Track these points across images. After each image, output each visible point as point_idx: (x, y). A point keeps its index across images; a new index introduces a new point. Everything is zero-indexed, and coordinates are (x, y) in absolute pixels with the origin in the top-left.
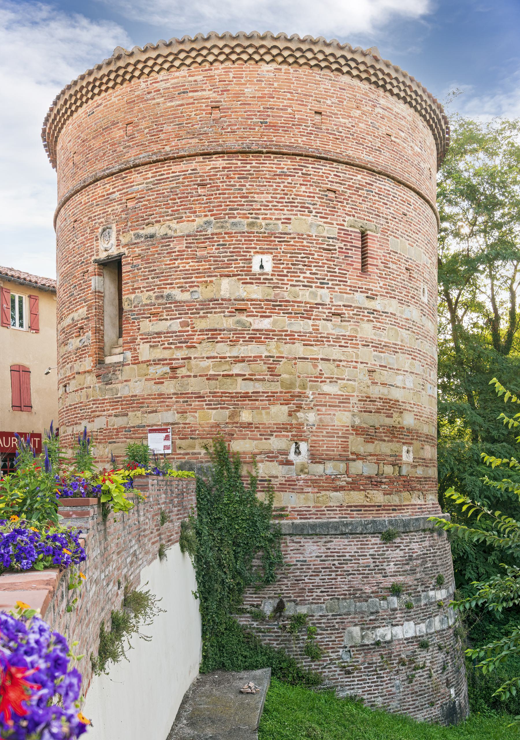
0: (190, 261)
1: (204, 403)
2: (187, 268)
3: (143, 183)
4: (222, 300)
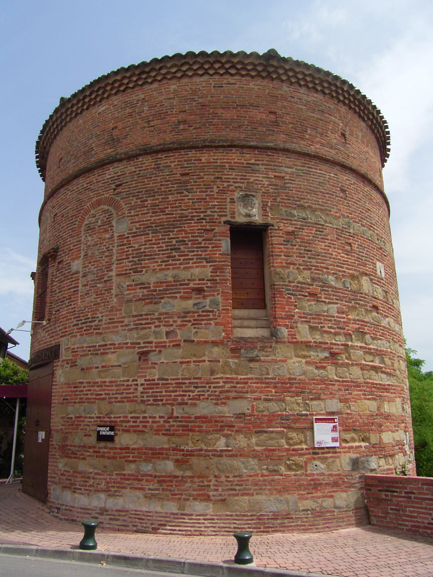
0: (340, 251)
1: (361, 393)
2: (339, 257)
3: (292, 168)
4: (366, 294)
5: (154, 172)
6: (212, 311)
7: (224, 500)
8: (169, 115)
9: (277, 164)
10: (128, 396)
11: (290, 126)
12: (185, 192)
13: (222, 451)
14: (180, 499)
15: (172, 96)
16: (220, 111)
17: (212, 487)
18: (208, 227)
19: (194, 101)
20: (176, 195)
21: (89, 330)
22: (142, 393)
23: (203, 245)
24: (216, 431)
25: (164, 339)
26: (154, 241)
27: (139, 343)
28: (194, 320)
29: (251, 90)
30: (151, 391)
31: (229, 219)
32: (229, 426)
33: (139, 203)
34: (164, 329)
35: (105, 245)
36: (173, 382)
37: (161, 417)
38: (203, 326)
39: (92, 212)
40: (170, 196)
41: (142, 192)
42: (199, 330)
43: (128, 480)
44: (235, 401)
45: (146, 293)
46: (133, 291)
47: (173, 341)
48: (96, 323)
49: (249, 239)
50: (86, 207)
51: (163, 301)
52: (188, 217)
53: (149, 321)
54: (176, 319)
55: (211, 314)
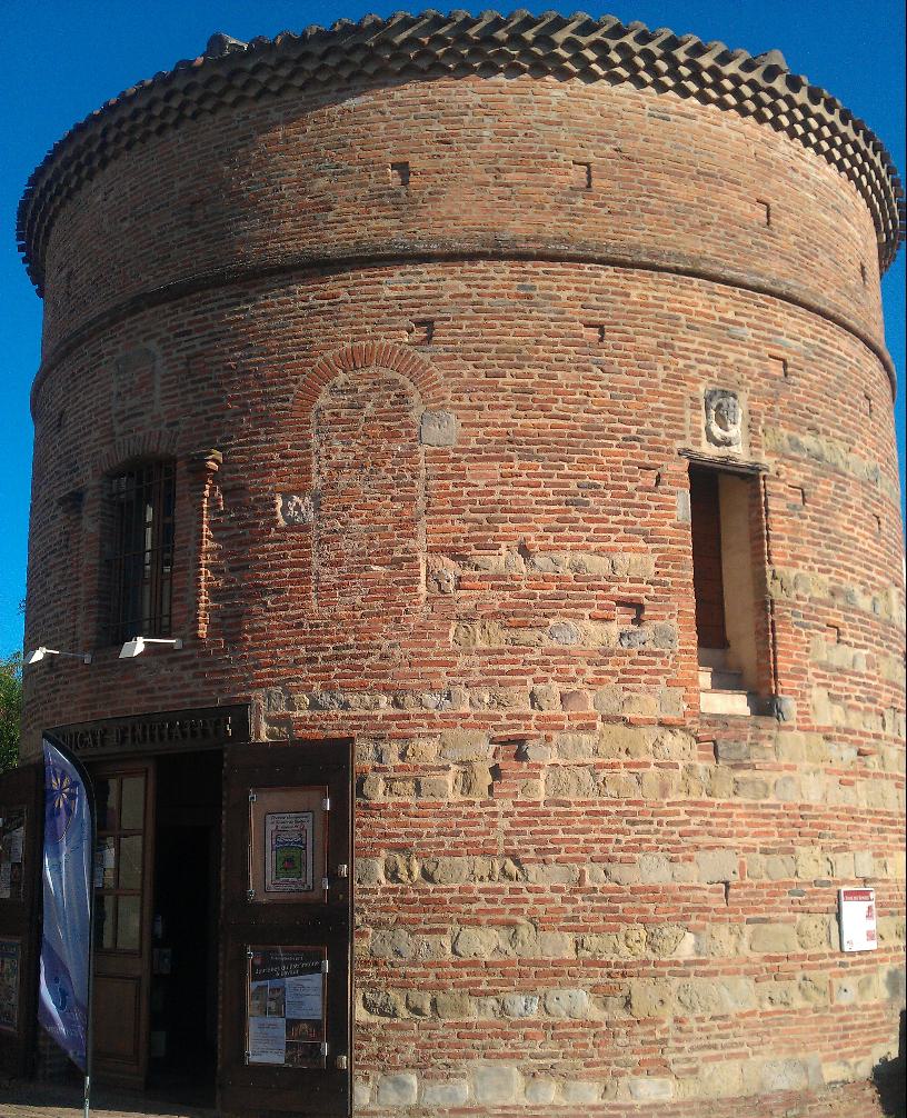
5: (519, 306)
6: (660, 654)
7: (694, 1071)
8: (552, 165)
9: (772, 326)
10: (473, 839)
11: (793, 238)
12: (594, 367)
13: (687, 963)
14: (603, 1075)
15: (553, 116)
16: (665, 180)
17: (672, 1044)
18: (647, 461)
19: (607, 142)
20: (574, 372)
22: (507, 833)
23: (636, 500)
24: (675, 919)
25: (557, 710)
26: (524, 479)
27: (498, 718)
28: (624, 672)
29: (721, 138)
30: (528, 829)
31: (690, 446)
32: (700, 910)
34: (557, 688)
35: (393, 470)
36: (583, 809)
37: (555, 890)
38: (643, 685)
39: (342, 377)
40: (559, 374)
41: (489, 351)
42: (634, 695)
43: (480, 1037)
44: (710, 854)
47: (578, 717)
49: (721, 494)
50: (320, 359)
51: (552, 622)
52: (602, 429)
53: (518, 667)
54: (584, 666)
55: (658, 660)
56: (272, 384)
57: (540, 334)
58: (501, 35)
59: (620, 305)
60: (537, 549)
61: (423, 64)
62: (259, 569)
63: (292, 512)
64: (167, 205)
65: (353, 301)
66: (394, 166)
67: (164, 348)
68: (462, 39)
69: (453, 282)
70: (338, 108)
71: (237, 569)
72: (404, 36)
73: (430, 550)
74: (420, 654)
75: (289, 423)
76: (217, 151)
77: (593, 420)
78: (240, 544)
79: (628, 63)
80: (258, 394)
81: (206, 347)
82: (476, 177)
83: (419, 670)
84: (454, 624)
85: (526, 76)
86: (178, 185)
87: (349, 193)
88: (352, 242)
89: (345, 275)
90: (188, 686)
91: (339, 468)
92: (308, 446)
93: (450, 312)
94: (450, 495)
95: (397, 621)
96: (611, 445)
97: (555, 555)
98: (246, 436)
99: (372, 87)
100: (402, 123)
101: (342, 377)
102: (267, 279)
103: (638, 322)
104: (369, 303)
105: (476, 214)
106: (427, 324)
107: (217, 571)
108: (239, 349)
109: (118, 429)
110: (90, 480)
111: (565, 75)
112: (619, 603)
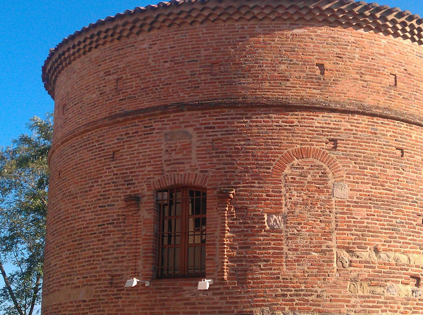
5: (372, 138)
12: (400, 168)
15: (382, 52)
21: (304, 305)
23: (416, 230)
26: (376, 217)
33: (358, 169)
39: (296, 161)
40: (388, 170)
41: (360, 156)
45: (371, 273)
46: (358, 269)
48: (314, 297)
50: (285, 151)
51: (388, 284)
52: (403, 197)
54: (400, 305)
56: (261, 160)
57: (380, 151)
58: (367, 13)
59: (408, 141)
60: (381, 250)
61: (332, 20)
62: (256, 249)
63: (272, 223)
64: (197, 61)
65: (301, 126)
66: (317, 65)
67: (198, 133)
68: (351, 12)
69: (344, 123)
70: (290, 32)
71: (244, 248)
72: (327, 6)
73: (338, 247)
74: (335, 296)
75: (270, 180)
76: (227, 41)
77: (400, 192)
78: (245, 235)
79: (412, 33)
80: (254, 164)
81: (223, 136)
82: (353, 75)
83: (334, 303)
84: (349, 283)
85: (372, 31)
86: (203, 53)
87: (297, 74)
88: (299, 98)
89: (297, 113)
90: (216, 303)
91: (295, 204)
92: (281, 192)
93: (344, 136)
94: (346, 222)
95: (324, 279)
96: (407, 204)
97: (389, 254)
98: (247, 183)
99: (307, 25)
100: (321, 45)
101: (296, 161)
102: (257, 109)
103: (415, 149)
104: (308, 128)
105: (352, 93)
106: (334, 141)
107: (232, 247)
108: (244, 140)
109: (166, 169)
110: (144, 190)
111: (387, 33)
112: (412, 277)
